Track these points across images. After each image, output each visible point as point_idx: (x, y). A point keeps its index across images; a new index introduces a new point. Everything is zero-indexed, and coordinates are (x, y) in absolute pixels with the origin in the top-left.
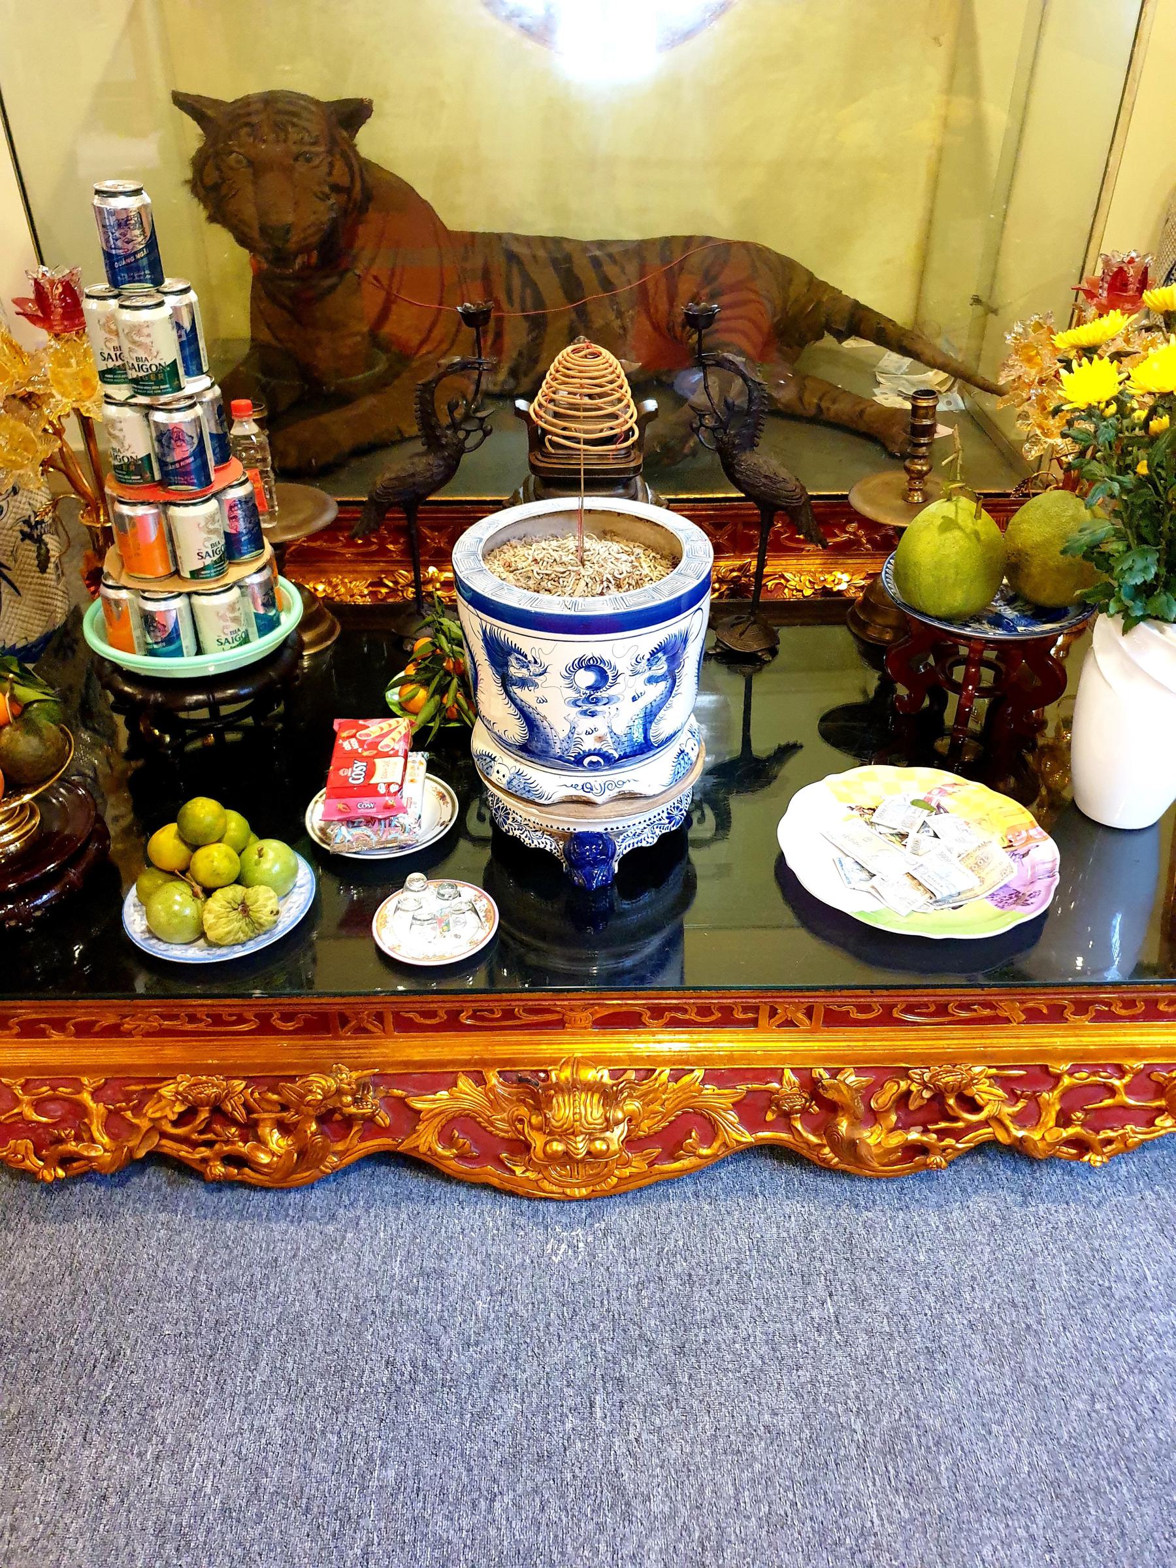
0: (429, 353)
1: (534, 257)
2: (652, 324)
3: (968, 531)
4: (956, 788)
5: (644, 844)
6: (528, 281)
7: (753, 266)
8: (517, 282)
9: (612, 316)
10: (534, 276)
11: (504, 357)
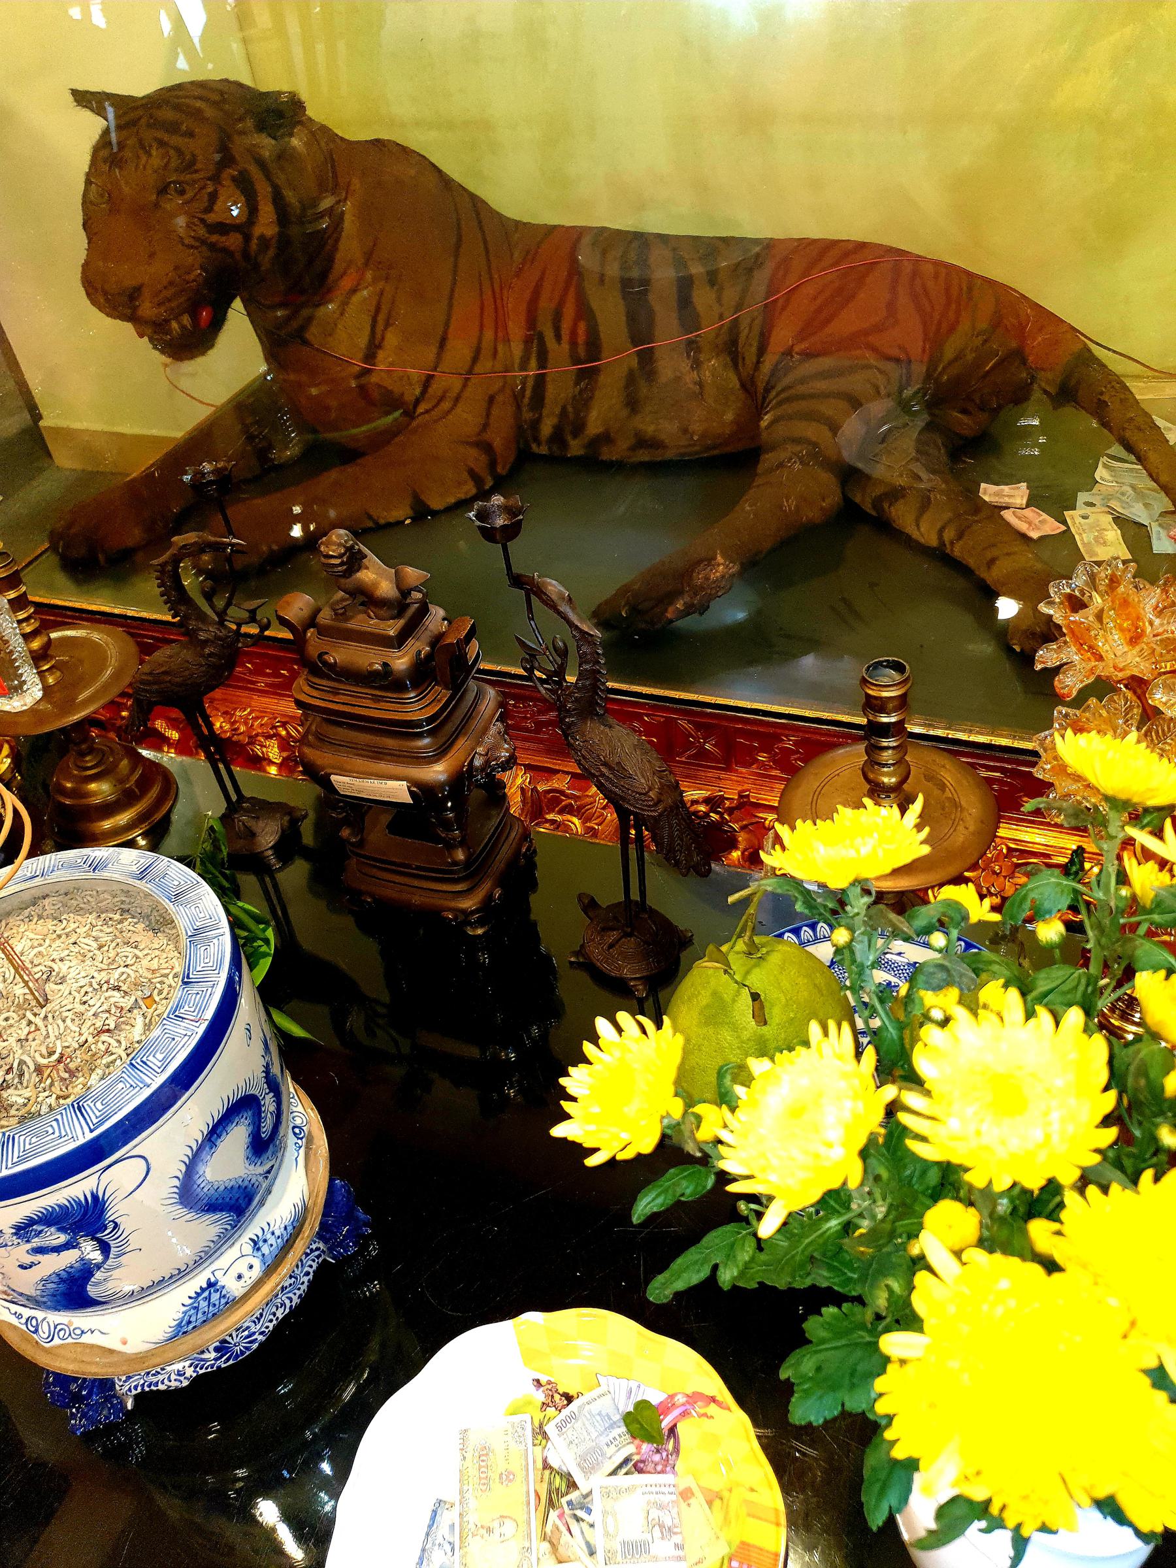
0: (427, 412)
1: (602, 279)
2: (740, 380)
3: (746, 1035)
4: (712, 1409)
5: (161, 1387)
6: (585, 312)
7: (891, 306)
8: (569, 311)
9: (685, 365)
10: (595, 304)
11: (545, 412)
